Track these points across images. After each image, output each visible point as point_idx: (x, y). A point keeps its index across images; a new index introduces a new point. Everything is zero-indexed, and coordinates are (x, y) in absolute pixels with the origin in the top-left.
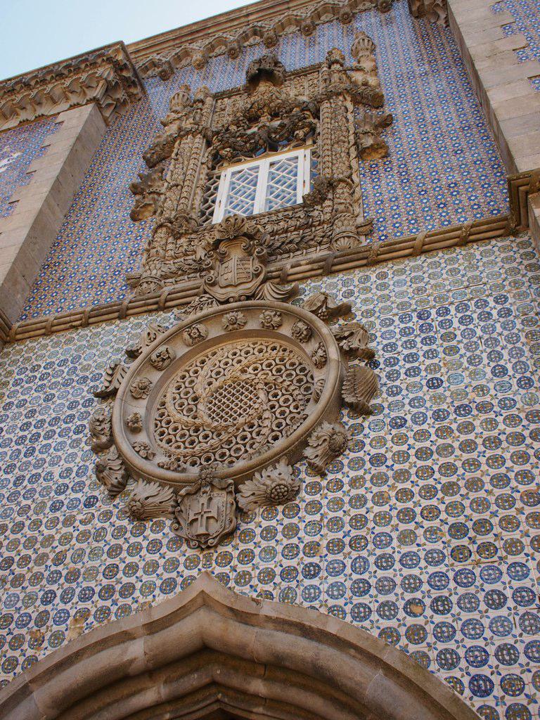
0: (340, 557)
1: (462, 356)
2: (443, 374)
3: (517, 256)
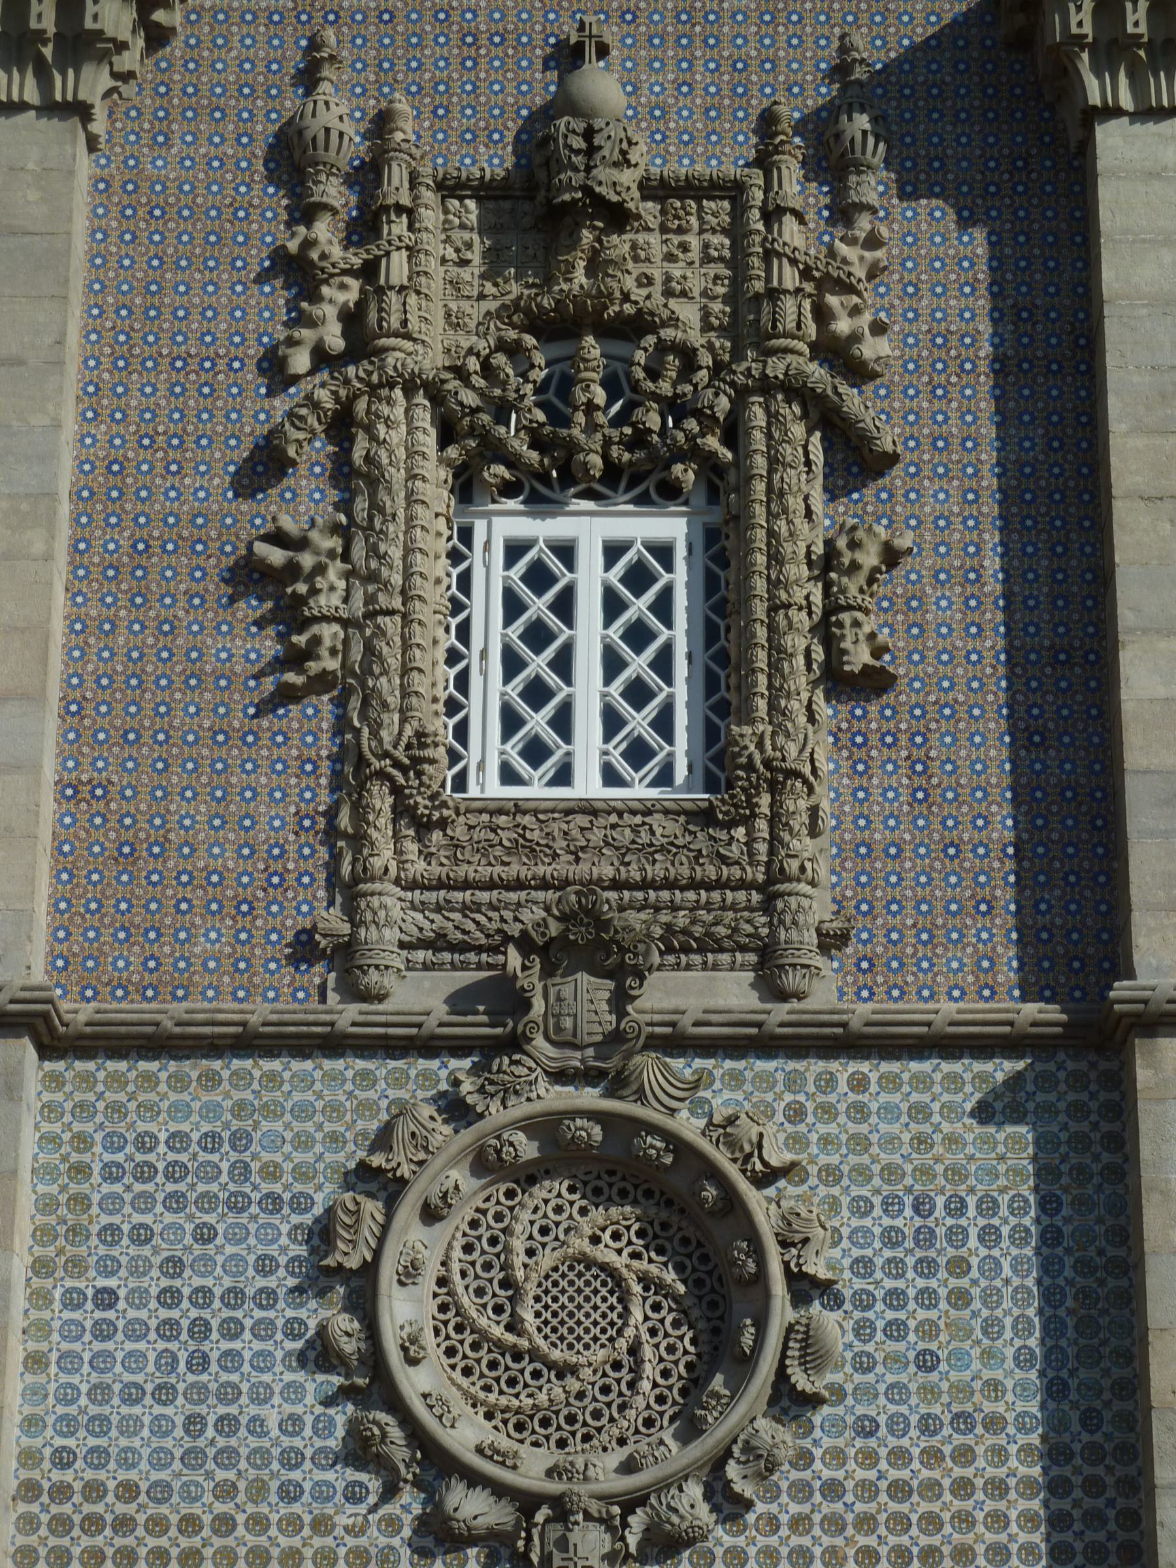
1: (975, 1314)
2: (941, 1345)
3: (1093, 1105)
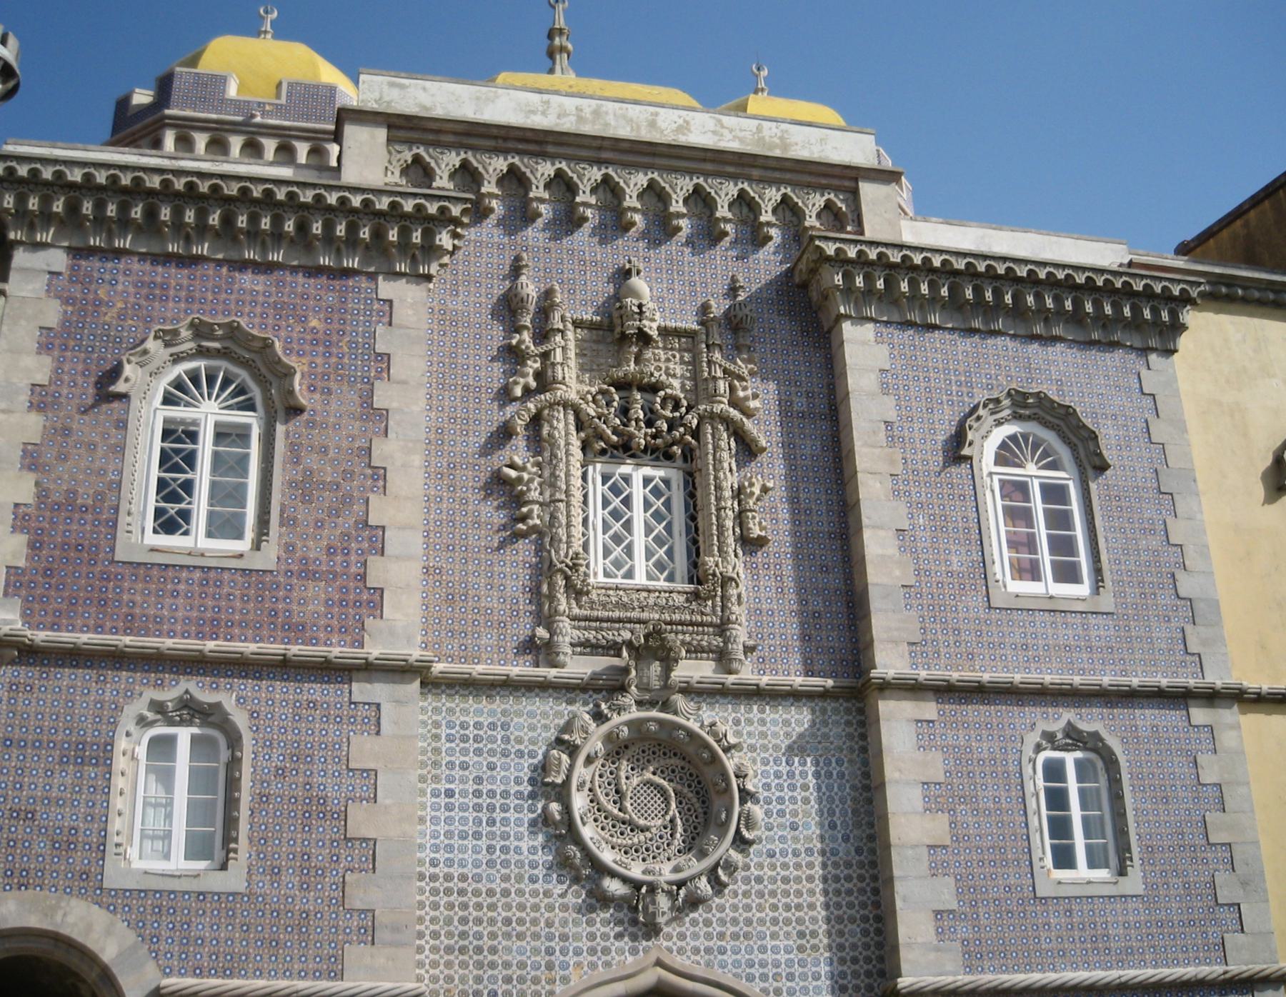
0: (738, 943)
2: (799, 820)
